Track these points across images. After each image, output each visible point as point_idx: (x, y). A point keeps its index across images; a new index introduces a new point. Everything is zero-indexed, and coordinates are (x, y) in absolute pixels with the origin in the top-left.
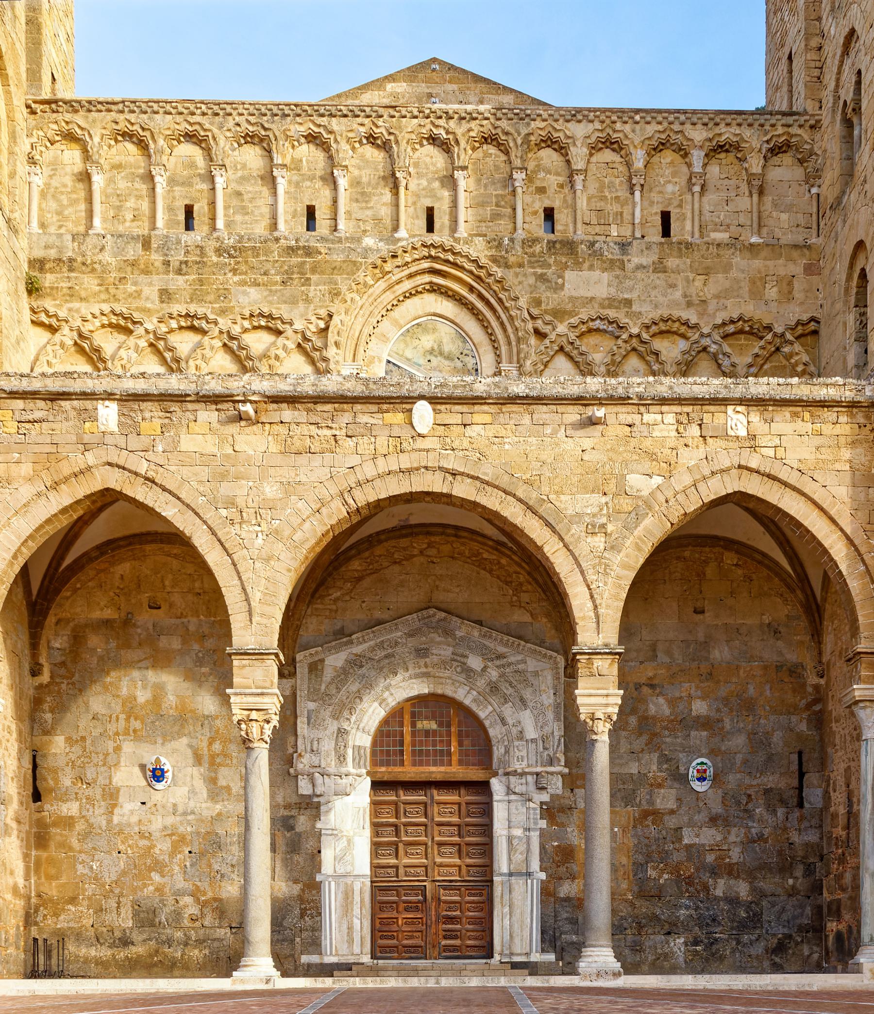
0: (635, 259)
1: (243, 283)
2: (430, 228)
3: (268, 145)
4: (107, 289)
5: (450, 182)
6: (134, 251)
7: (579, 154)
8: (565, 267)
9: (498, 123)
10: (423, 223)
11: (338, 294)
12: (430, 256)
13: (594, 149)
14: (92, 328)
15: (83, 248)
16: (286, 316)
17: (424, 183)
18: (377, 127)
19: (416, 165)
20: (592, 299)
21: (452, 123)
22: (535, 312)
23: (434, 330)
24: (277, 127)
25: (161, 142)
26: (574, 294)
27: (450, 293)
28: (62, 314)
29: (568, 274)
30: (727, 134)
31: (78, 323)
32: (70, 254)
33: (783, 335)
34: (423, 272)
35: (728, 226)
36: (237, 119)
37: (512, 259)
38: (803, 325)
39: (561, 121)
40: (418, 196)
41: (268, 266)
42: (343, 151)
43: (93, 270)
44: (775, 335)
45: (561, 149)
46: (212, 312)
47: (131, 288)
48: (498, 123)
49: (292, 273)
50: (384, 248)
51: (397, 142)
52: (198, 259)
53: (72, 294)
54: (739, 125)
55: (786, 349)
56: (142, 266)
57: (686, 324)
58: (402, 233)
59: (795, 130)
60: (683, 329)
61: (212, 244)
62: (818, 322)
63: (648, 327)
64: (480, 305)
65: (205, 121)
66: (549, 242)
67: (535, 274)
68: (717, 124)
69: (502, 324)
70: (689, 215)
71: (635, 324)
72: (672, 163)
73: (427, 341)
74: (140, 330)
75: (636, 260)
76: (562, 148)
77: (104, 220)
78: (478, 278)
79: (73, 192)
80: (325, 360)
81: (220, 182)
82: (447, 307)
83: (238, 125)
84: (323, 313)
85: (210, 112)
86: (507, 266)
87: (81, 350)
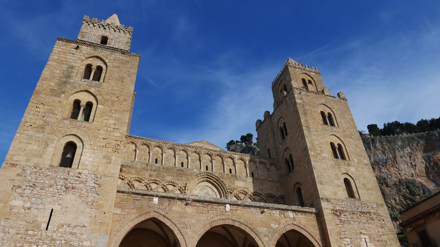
1: (168, 175)
2: (207, 169)
3: (175, 150)
4: (137, 173)
5: (211, 162)
6: (144, 166)
8: (235, 180)
9: (220, 153)
11: (188, 180)
12: (207, 175)
13: (238, 160)
14: (132, 180)
15: (133, 164)
16: (177, 183)
17: (206, 161)
18: (197, 150)
19: (204, 158)
20: (241, 187)
21: (212, 152)
22: (230, 188)
23: (207, 189)
24: (177, 147)
25: (152, 147)
26: (237, 185)
27: (210, 182)
28: (126, 176)
29: (236, 182)
31: (129, 179)
33: (278, 198)
35: (264, 176)
36: (169, 145)
37: (224, 177)
38: (281, 196)
39: (232, 154)
40: (204, 163)
41: (174, 172)
42: (190, 153)
43: (135, 168)
44: (276, 197)
46: (160, 180)
47: (143, 173)
48: (220, 153)
49: (179, 174)
50: (198, 172)
51: (201, 153)
52: (158, 169)
53: (129, 173)
54: (265, 159)
55: (279, 200)
56: (146, 169)
57: (259, 193)
58: (202, 170)
59: (274, 162)
60: (259, 194)
61: (162, 167)
62: (284, 196)
64: (217, 185)
65: (162, 144)
66: (231, 175)
67: (229, 181)
68: (261, 159)
69: (222, 190)
70: (257, 173)
71: (250, 192)
72: (252, 164)
75: (248, 180)
76: (232, 159)
77: (138, 159)
78: (217, 180)
79: (131, 153)
80: (185, 193)
81: (164, 155)
82: (210, 185)
83: (169, 146)
84: (185, 183)
85: (164, 143)
86: (223, 178)
87: (129, 185)
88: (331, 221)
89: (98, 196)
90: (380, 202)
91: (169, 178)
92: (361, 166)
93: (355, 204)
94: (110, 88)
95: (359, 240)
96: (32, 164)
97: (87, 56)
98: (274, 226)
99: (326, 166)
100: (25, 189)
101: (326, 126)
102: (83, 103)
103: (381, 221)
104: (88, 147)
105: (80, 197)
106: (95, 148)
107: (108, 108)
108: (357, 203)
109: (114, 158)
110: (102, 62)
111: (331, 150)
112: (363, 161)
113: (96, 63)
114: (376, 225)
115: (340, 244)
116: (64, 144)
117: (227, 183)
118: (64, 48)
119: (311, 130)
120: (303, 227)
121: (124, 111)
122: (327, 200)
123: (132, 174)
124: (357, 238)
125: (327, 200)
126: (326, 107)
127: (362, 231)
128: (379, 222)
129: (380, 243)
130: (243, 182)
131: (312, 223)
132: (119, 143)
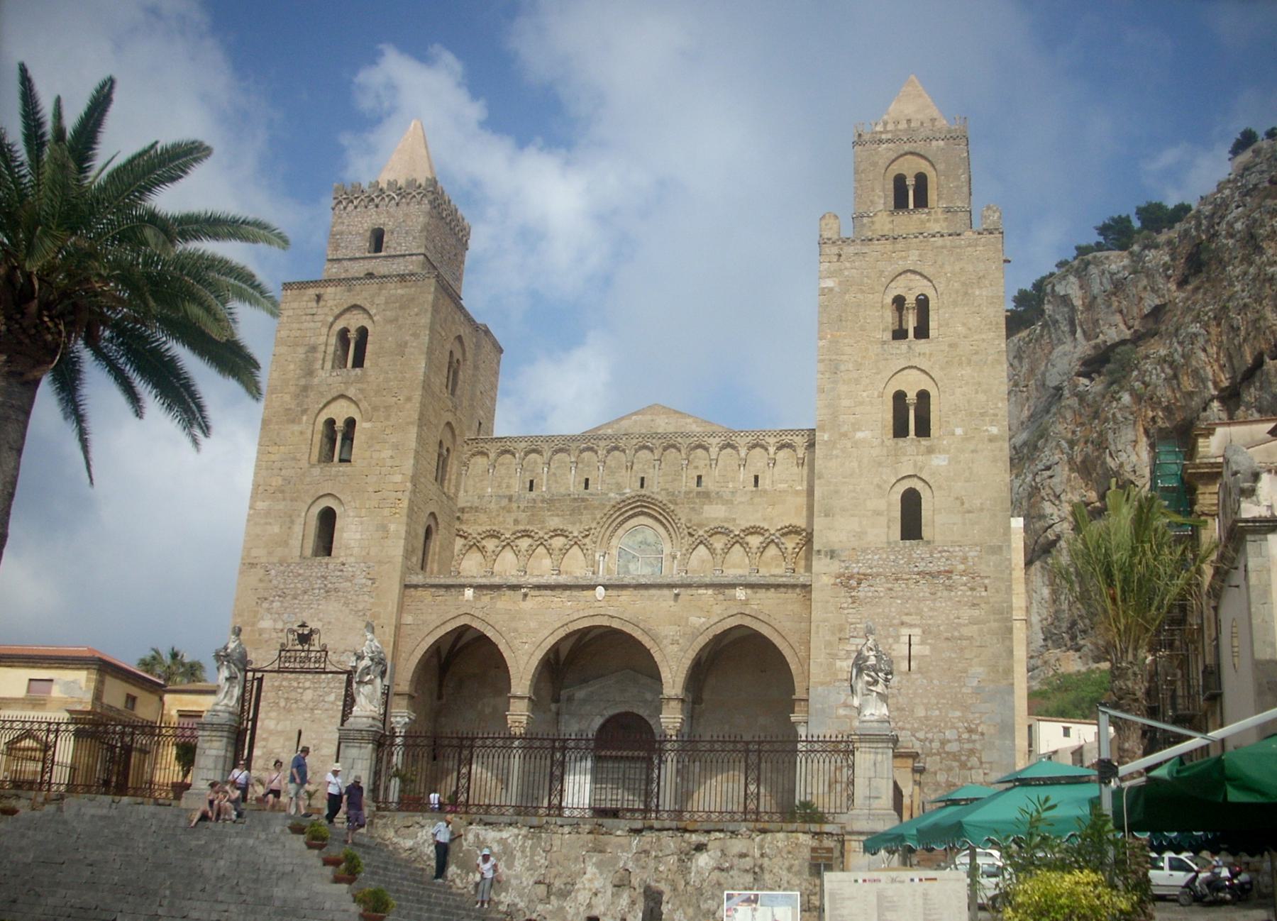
0: (739, 498)
1: (552, 515)
2: (642, 486)
6: (505, 502)
7: (714, 451)
10: (639, 484)
11: (595, 519)
20: (716, 519)
24: (573, 445)
28: (470, 531)
29: (706, 507)
30: (787, 439)
32: (476, 504)
34: (637, 507)
37: (678, 501)
45: (707, 449)
47: (501, 519)
50: (619, 498)
61: (540, 498)
63: (744, 531)
64: (664, 521)
73: (639, 538)
74: (503, 537)
75: (739, 499)
78: (664, 510)
82: (649, 521)
86: (676, 504)
88: (827, 602)
89: (372, 600)
91: (555, 522)
92: (972, 447)
93: (911, 555)
94: (381, 379)
95: (891, 640)
96: (275, 560)
97: (337, 311)
98: (697, 621)
99: (855, 464)
101: (897, 343)
102: (340, 424)
103: (979, 589)
104: (352, 514)
105: (346, 604)
107: (379, 425)
108: (916, 549)
109: (392, 527)
110: (365, 316)
111: (889, 416)
112: (987, 430)
113: (354, 322)
114: (959, 602)
116: (315, 518)
117: (683, 514)
118: (295, 305)
119: (842, 368)
121: (408, 424)
122: (832, 554)
123: (481, 525)
124: (886, 637)
126: (918, 277)
127: (905, 618)
128: (969, 593)
130: (724, 508)
131: (790, 608)
132: (399, 495)
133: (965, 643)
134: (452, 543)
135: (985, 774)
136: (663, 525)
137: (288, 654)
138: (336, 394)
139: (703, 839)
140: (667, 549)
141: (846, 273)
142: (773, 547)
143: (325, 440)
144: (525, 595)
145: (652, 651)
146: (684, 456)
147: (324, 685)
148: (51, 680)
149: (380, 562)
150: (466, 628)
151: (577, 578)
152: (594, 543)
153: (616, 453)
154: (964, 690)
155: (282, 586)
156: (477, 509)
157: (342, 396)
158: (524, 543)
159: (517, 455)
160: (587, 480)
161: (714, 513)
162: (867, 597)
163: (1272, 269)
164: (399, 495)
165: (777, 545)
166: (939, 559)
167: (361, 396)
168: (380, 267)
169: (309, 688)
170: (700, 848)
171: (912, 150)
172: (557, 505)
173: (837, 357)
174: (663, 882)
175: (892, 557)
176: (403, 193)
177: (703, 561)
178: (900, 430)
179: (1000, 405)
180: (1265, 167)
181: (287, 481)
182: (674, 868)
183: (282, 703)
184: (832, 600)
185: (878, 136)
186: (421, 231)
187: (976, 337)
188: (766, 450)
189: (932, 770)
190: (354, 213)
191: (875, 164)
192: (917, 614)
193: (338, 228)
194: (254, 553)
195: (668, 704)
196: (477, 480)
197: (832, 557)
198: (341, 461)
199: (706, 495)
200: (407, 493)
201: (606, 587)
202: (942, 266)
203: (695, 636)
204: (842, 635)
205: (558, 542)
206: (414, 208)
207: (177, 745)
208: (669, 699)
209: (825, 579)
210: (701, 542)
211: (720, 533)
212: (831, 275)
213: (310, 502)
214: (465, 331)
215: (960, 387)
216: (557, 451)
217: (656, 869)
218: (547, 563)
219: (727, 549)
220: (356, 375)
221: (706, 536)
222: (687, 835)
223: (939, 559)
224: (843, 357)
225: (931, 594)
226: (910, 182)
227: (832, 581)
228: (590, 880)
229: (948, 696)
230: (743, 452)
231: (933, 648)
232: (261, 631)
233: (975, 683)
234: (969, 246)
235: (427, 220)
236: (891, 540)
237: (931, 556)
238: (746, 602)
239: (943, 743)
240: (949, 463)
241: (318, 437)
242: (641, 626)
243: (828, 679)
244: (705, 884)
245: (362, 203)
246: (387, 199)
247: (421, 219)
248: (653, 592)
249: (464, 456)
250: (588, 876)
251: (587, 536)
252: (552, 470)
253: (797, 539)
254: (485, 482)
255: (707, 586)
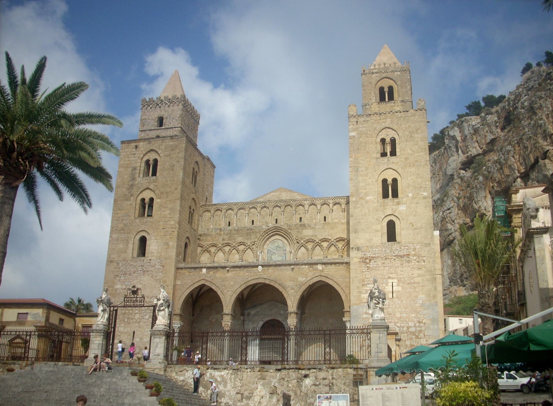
0: (317, 227)
2: (276, 222)
6: (218, 231)
7: (306, 207)
8: (303, 229)
10: (275, 222)
20: (308, 235)
22: (297, 238)
24: (247, 206)
28: (204, 244)
29: (304, 230)
30: (337, 201)
34: (275, 231)
37: (292, 228)
45: (303, 206)
47: (217, 239)
50: (267, 228)
64: (286, 237)
65: (233, 206)
74: (218, 246)
75: (318, 227)
78: (286, 232)
82: (280, 238)
86: (291, 230)
88: (357, 269)
90: (427, 242)
91: (240, 239)
93: (392, 248)
97: (144, 153)
98: (302, 279)
99: (367, 210)
100: (121, 277)
102: (147, 200)
105: (152, 277)
106: (158, 238)
109: (171, 244)
110: (157, 154)
111: (380, 190)
112: (422, 194)
113: (152, 157)
114: (413, 267)
115: (360, 290)
117: (294, 234)
118: (127, 150)
119: (360, 170)
120: (331, 277)
121: (176, 199)
122: (358, 249)
124: (383, 284)
125: (358, 249)
126: (391, 130)
127: (390, 275)
128: (417, 264)
129: (410, 285)
132: (173, 230)
133: (416, 285)
134: (196, 250)
135: (426, 340)
136: (286, 239)
137: (128, 299)
138: (145, 188)
139: (307, 372)
140: (288, 249)
141: (360, 129)
142: (333, 247)
143: (141, 207)
144: (228, 271)
145: (283, 293)
146: (294, 209)
147: (143, 312)
148: (27, 313)
149: (166, 259)
150: (203, 286)
151: (250, 262)
152: (257, 247)
153: (265, 209)
154: (416, 305)
155: (124, 270)
156: (206, 235)
157: (148, 188)
158: (227, 249)
159: (223, 211)
160: (253, 221)
161: (308, 233)
162: (373, 267)
163: (541, 122)
164: (173, 230)
165: (335, 246)
166: (404, 249)
167: (156, 188)
168: (162, 133)
169: (137, 313)
170: (306, 376)
171: (386, 76)
172: (241, 232)
173: (358, 165)
174: (291, 391)
175: (384, 249)
176: (171, 101)
177: (303, 254)
178: (385, 195)
179: (427, 183)
180: (536, 79)
181: (125, 225)
182: (295, 385)
183: (126, 320)
184: (359, 269)
185: (372, 71)
186: (179, 117)
187: (416, 155)
188: (329, 205)
189: (404, 339)
190: (150, 111)
191: (371, 83)
192: (395, 273)
193: (144, 117)
194: (112, 256)
195: (290, 315)
196: (206, 222)
197: (358, 251)
198: (148, 216)
199: (304, 226)
200: (177, 229)
201: (262, 266)
202: (401, 125)
203: (301, 286)
204: (363, 284)
205: (242, 248)
206: (176, 107)
207: (82, 340)
208: (291, 313)
209: (356, 260)
210: (302, 246)
211: (310, 241)
212: (354, 130)
213: (135, 234)
214: (199, 159)
215: (410, 176)
216: (240, 209)
217: (288, 386)
218: (237, 257)
219: (313, 249)
220: (153, 179)
221: (304, 243)
222: (300, 371)
223: (404, 249)
224: (360, 165)
225: (401, 264)
226: (386, 90)
227: (359, 260)
228: (260, 392)
229: (410, 308)
230: (319, 207)
231: (403, 288)
232: (116, 290)
233: (421, 302)
234: (412, 116)
235: (181, 112)
236: (383, 242)
237: (400, 248)
238: (322, 271)
239: (408, 328)
240: (407, 209)
241: (138, 206)
242: (278, 282)
243: (358, 302)
244: (309, 392)
245: (154, 106)
246: (164, 104)
247: (179, 112)
248: (283, 267)
249: (200, 212)
250: (259, 390)
251: (254, 244)
252: (238, 217)
253: (343, 243)
254: (210, 223)
255: (305, 264)
